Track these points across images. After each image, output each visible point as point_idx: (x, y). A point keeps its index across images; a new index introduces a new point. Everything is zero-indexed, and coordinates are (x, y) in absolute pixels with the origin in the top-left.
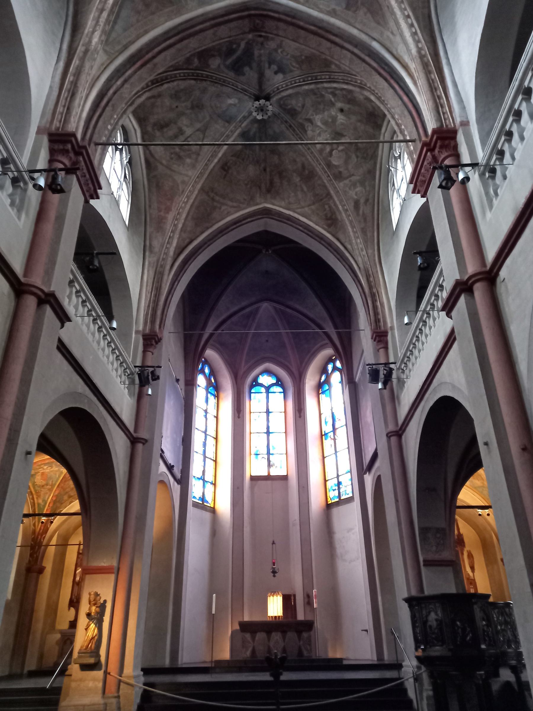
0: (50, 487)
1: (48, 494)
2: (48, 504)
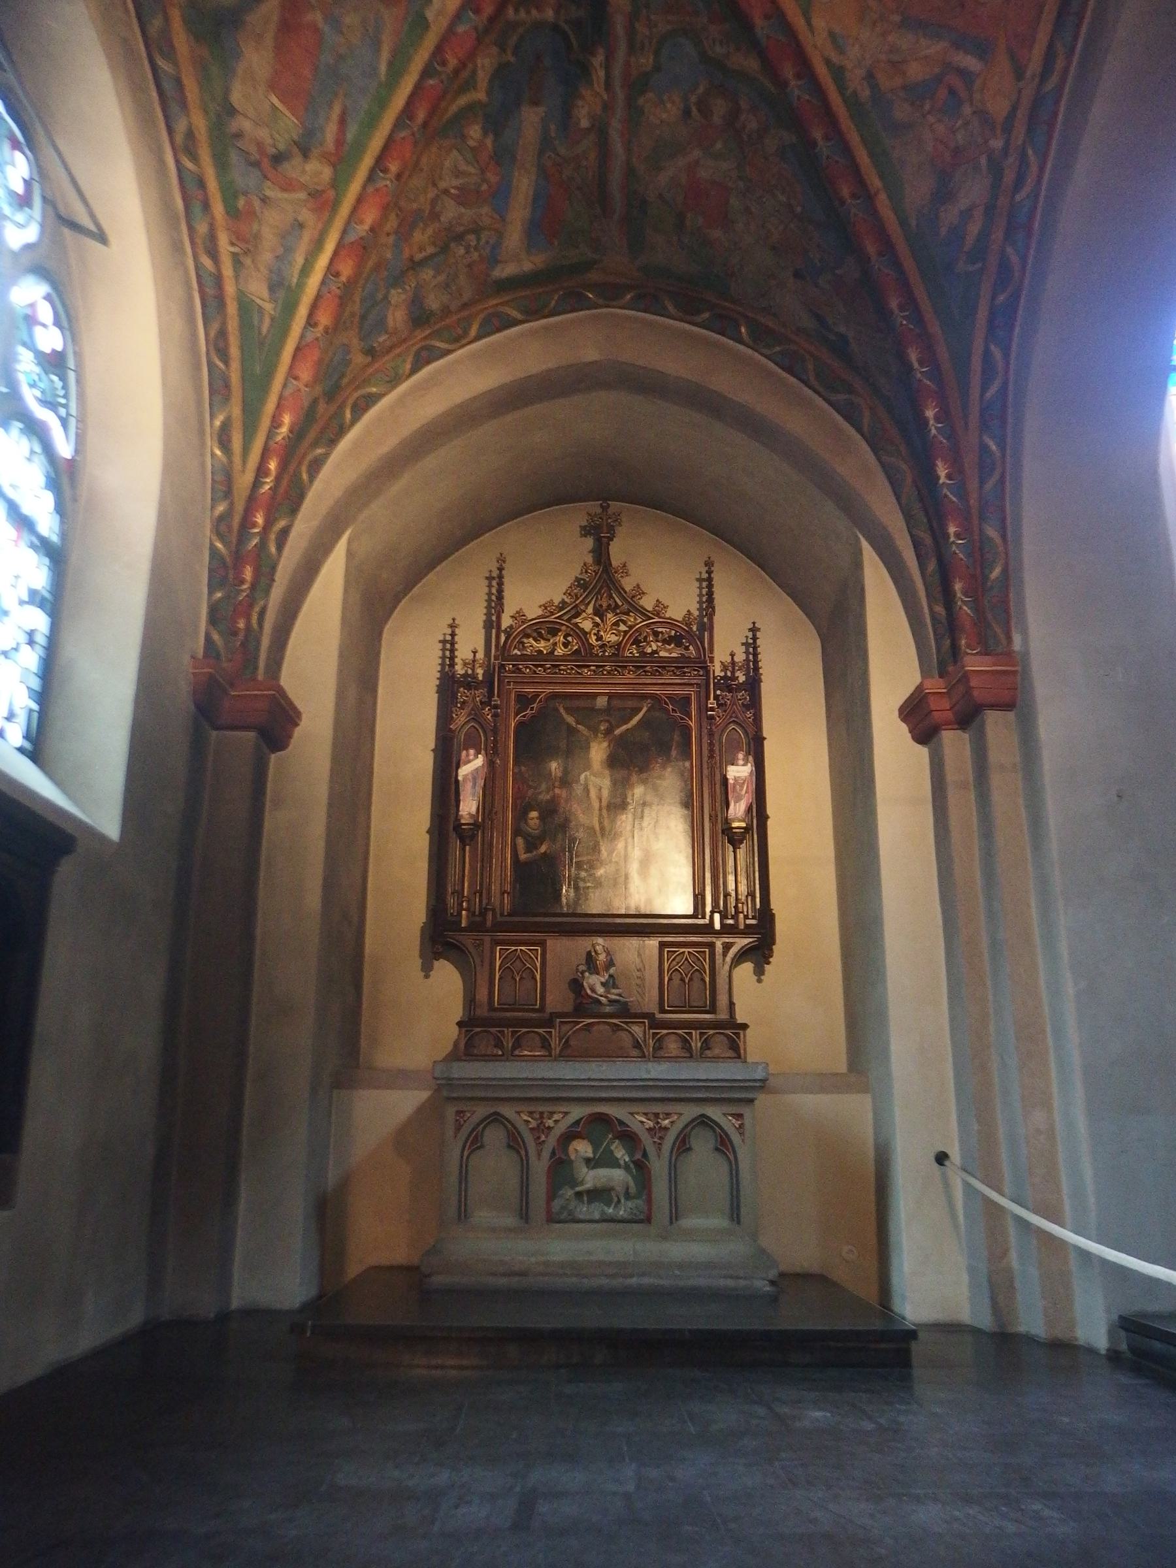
1: (307, 236)
2: (303, 311)
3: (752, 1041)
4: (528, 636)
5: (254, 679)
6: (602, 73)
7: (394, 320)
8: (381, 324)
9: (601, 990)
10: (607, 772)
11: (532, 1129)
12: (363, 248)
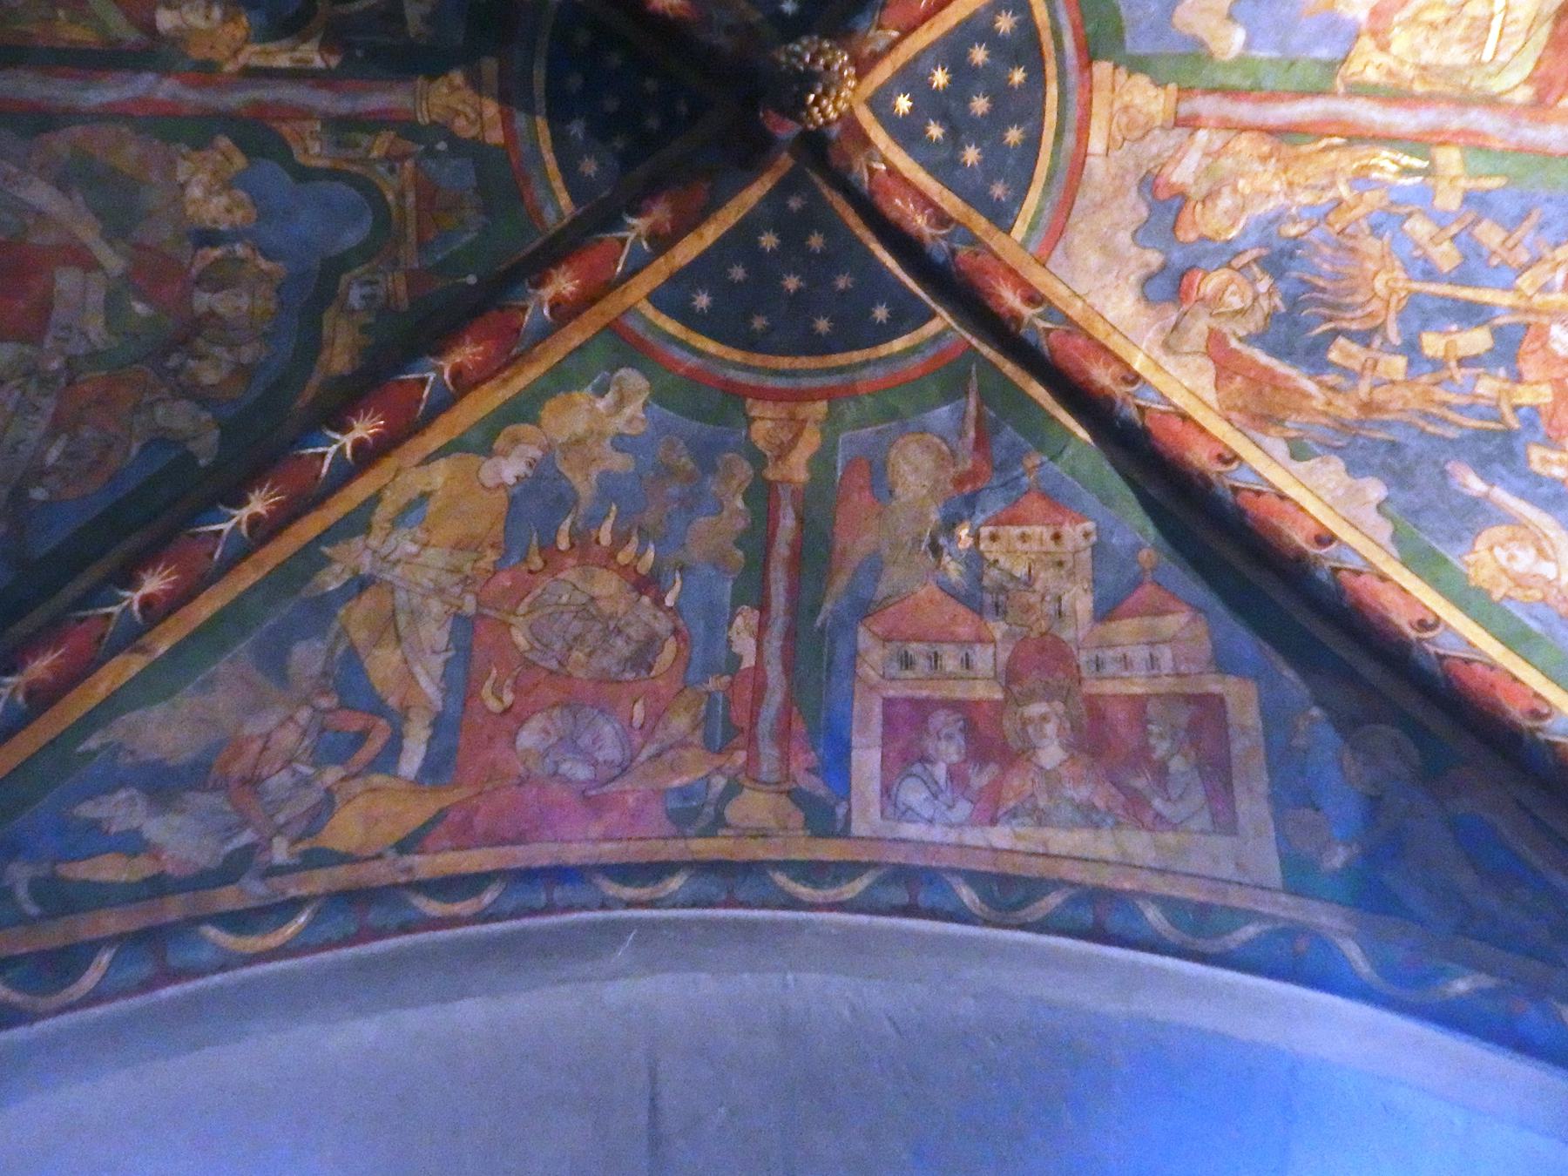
6: (283, 61)
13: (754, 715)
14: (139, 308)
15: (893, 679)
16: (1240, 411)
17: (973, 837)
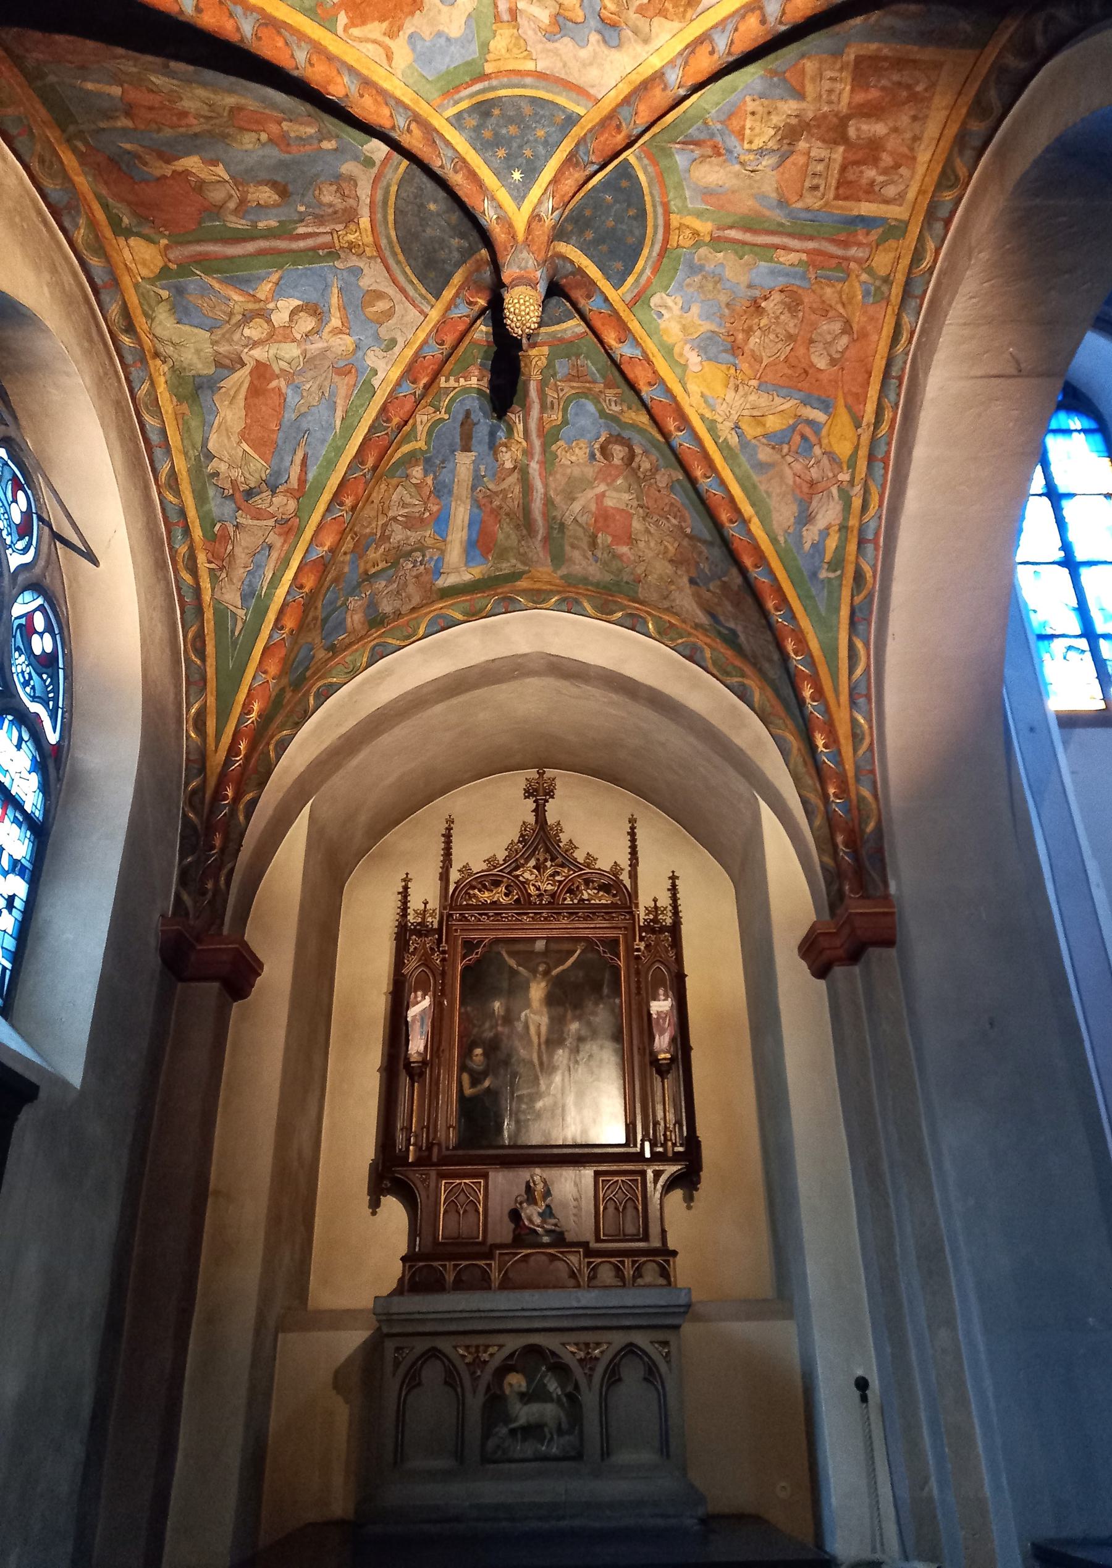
0: (292, 505)
2: (271, 616)
3: (683, 1268)
4: (474, 888)
5: (220, 934)
7: (352, 621)
8: (341, 625)
9: (537, 1220)
10: (545, 1010)
11: (468, 1364)
12: (323, 566)
13: (832, 256)
14: (619, 482)
15: (824, 195)
16: (685, 11)
17: (921, 170)
